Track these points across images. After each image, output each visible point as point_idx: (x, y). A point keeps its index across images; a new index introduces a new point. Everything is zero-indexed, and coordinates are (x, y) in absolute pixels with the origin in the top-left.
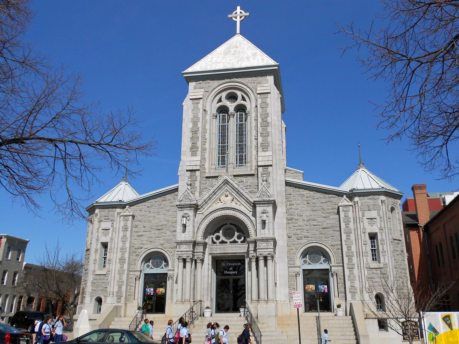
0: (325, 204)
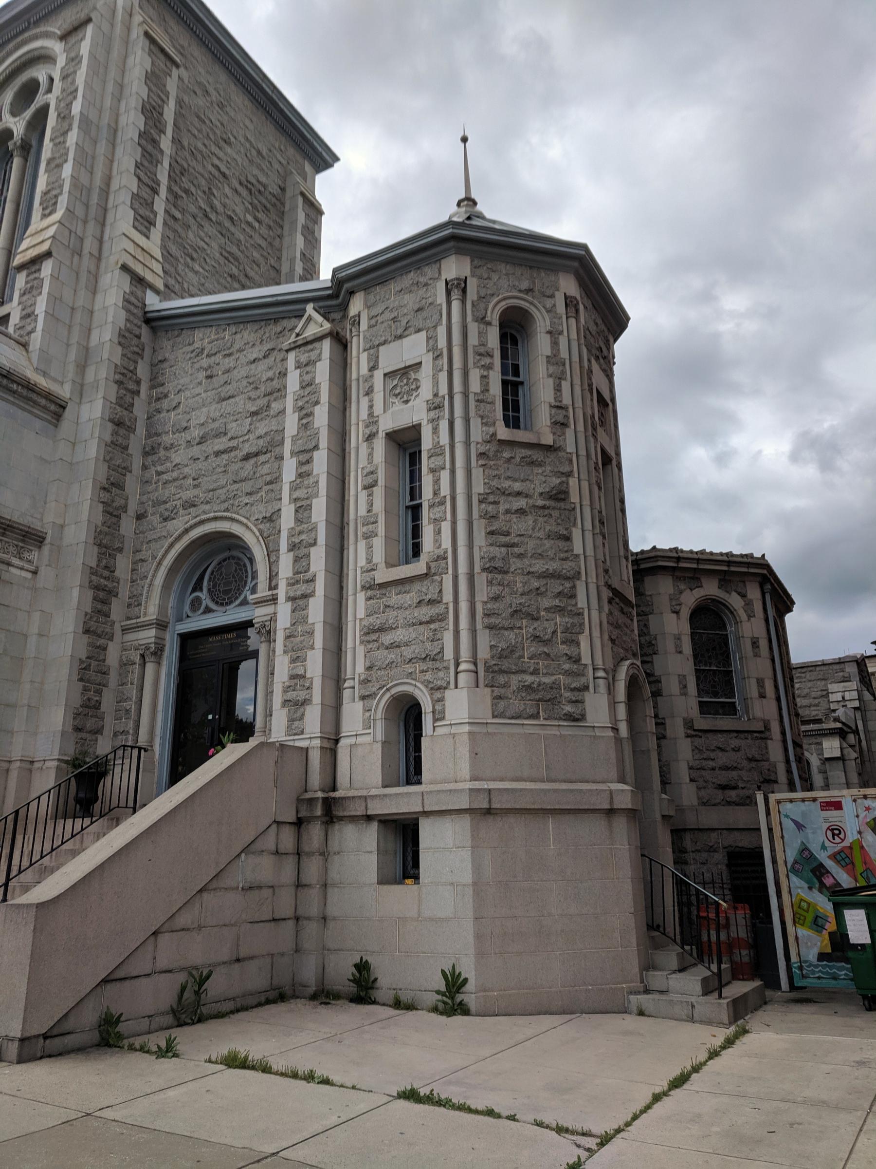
0: (262, 366)
